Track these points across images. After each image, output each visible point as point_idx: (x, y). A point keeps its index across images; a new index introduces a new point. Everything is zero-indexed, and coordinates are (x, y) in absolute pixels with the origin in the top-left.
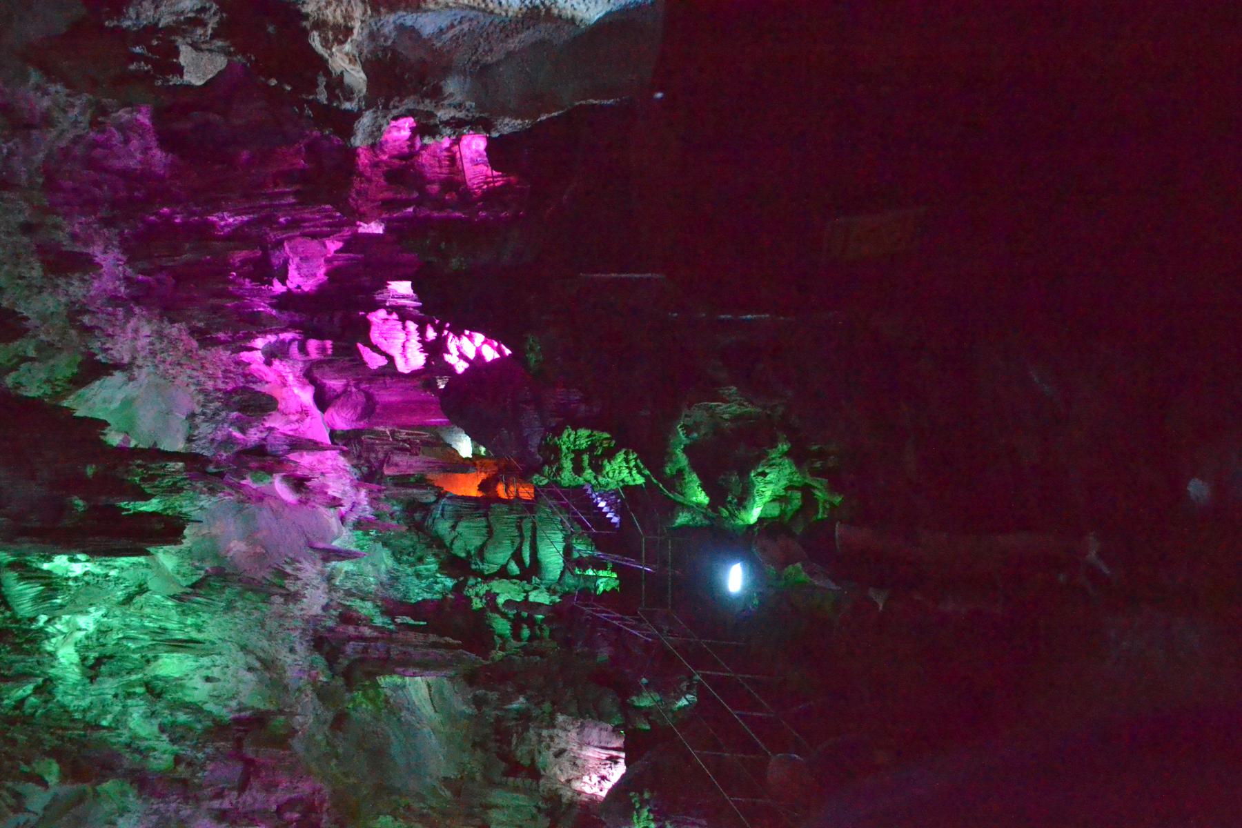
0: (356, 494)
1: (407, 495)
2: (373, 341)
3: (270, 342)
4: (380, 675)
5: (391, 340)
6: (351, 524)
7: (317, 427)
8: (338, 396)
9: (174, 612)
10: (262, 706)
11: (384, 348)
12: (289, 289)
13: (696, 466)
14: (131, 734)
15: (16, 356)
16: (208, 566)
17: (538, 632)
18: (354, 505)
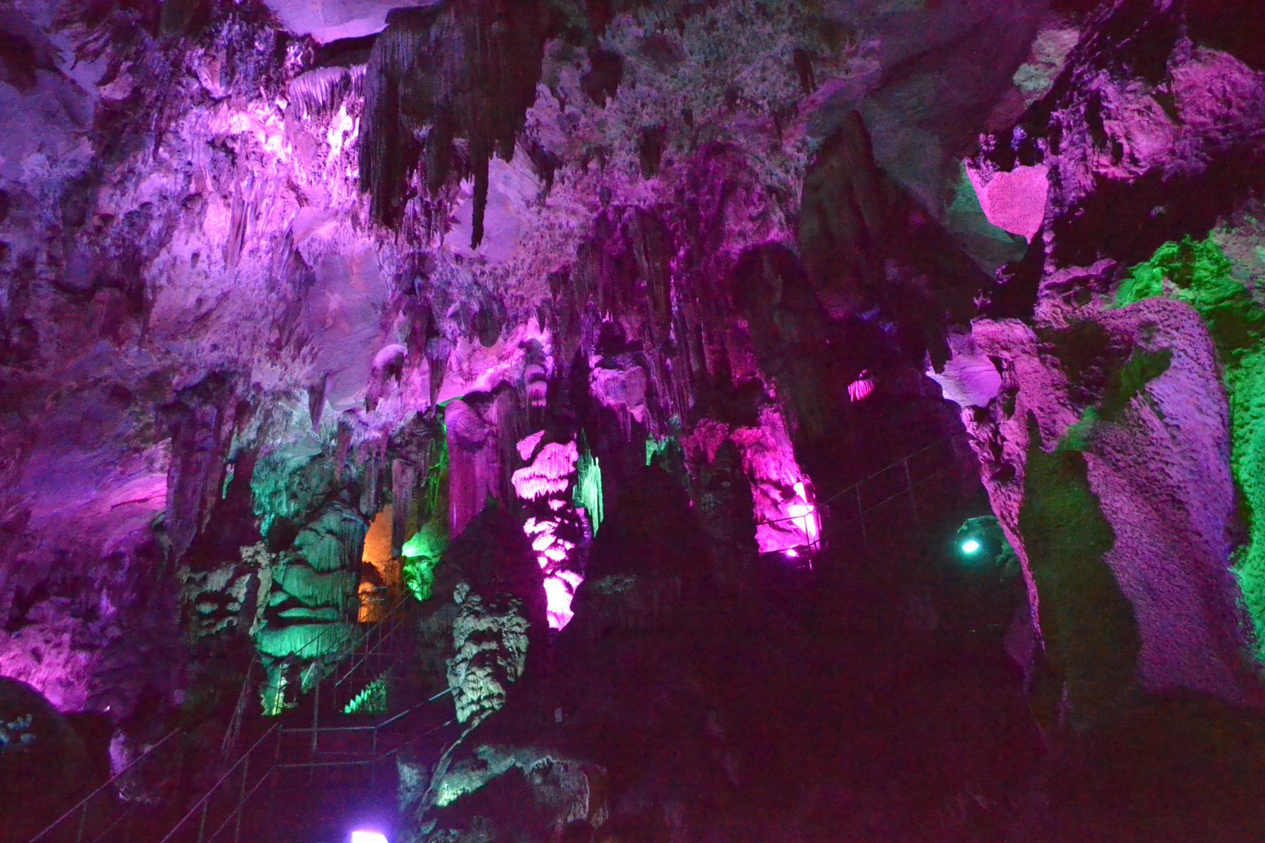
1: (369, 486)
2: (548, 446)
4: (173, 442)
6: (346, 420)
7: (453, 391)
8: (479, 415)
9: (276, 228)
10: (156, 311)
11: (540, 456)
12: (591, 370)
13: (492, 784)
14: (144, 175)
15: (566, 96)
16: (317, 269)
17: (205, 623)
18: (365, 424)
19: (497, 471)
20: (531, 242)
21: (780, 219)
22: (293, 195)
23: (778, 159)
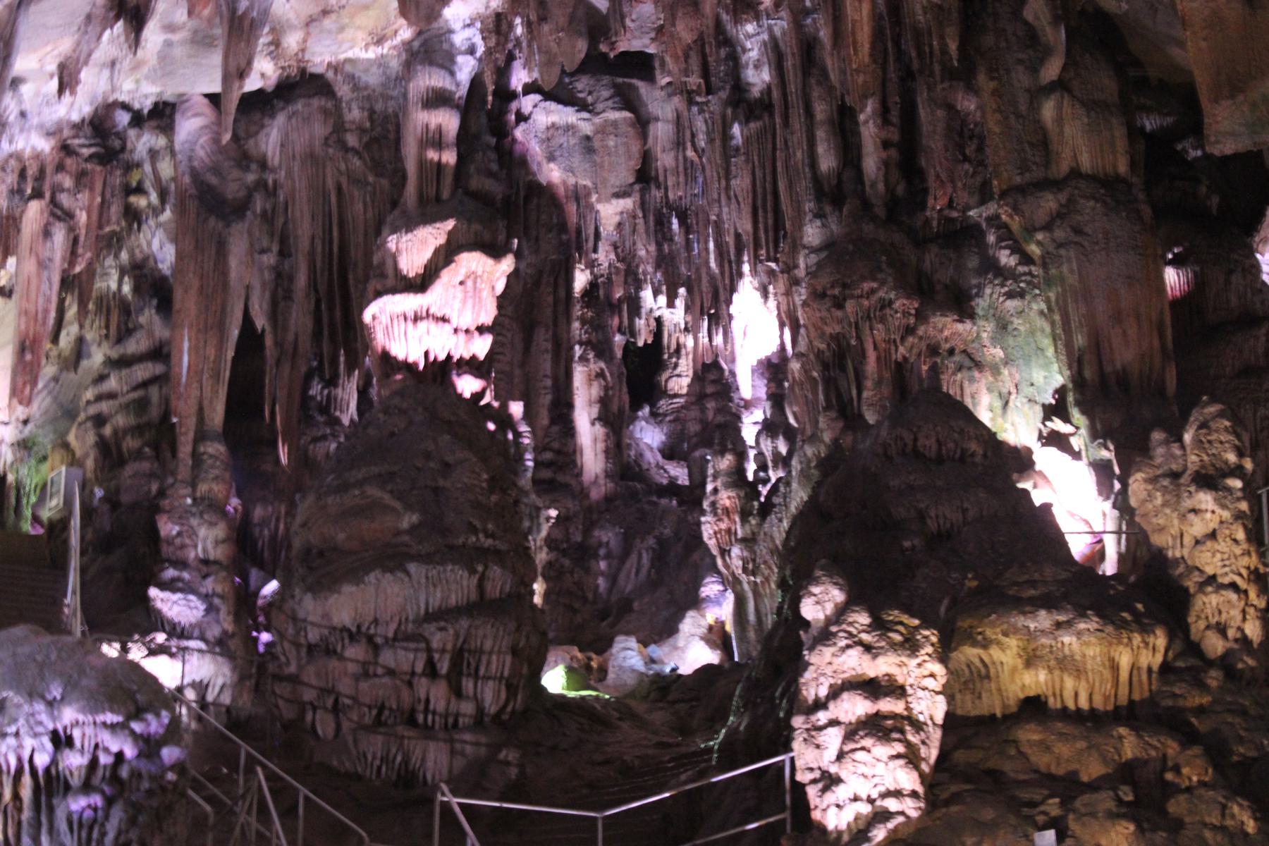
0: (41, 126)
3: (451, 31)
5: (460, 295)
12: (513, 96)
18: (23, 114)
19: (267, 275)
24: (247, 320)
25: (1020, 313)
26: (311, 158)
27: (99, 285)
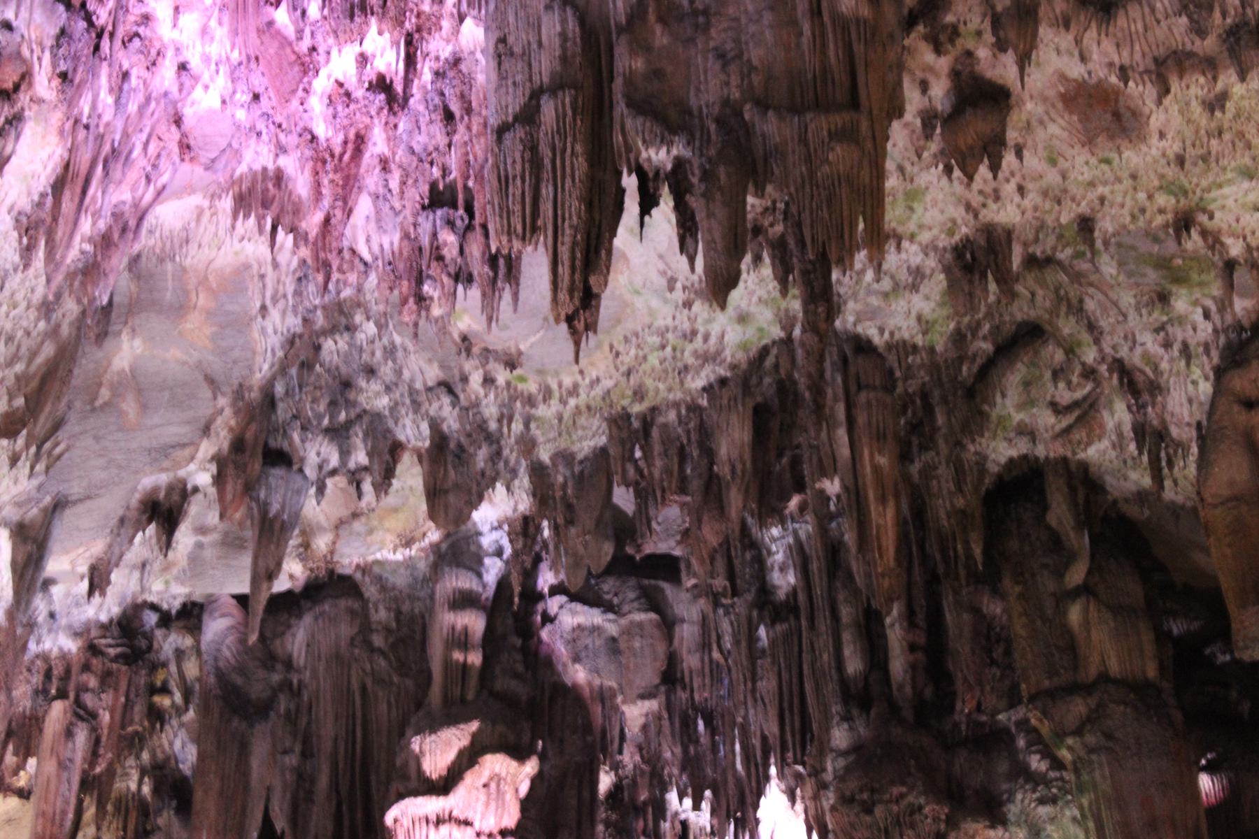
0: (70, 627)
3: (479, 534)
5: (483, 798)
12: (540, 597)
18: (52, 615)
20: (633, 352)
21: (1118, 427)
22: (175, 134)
23: (1158, 316)
24: (267, 822)
25: (1052, 820)
26: (337, 658)
27: (119, 785)
